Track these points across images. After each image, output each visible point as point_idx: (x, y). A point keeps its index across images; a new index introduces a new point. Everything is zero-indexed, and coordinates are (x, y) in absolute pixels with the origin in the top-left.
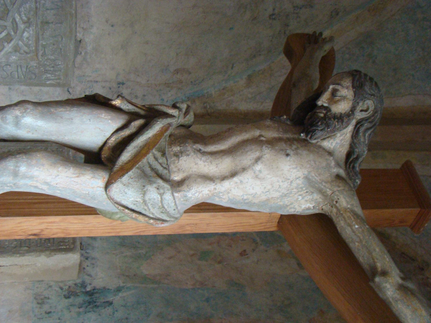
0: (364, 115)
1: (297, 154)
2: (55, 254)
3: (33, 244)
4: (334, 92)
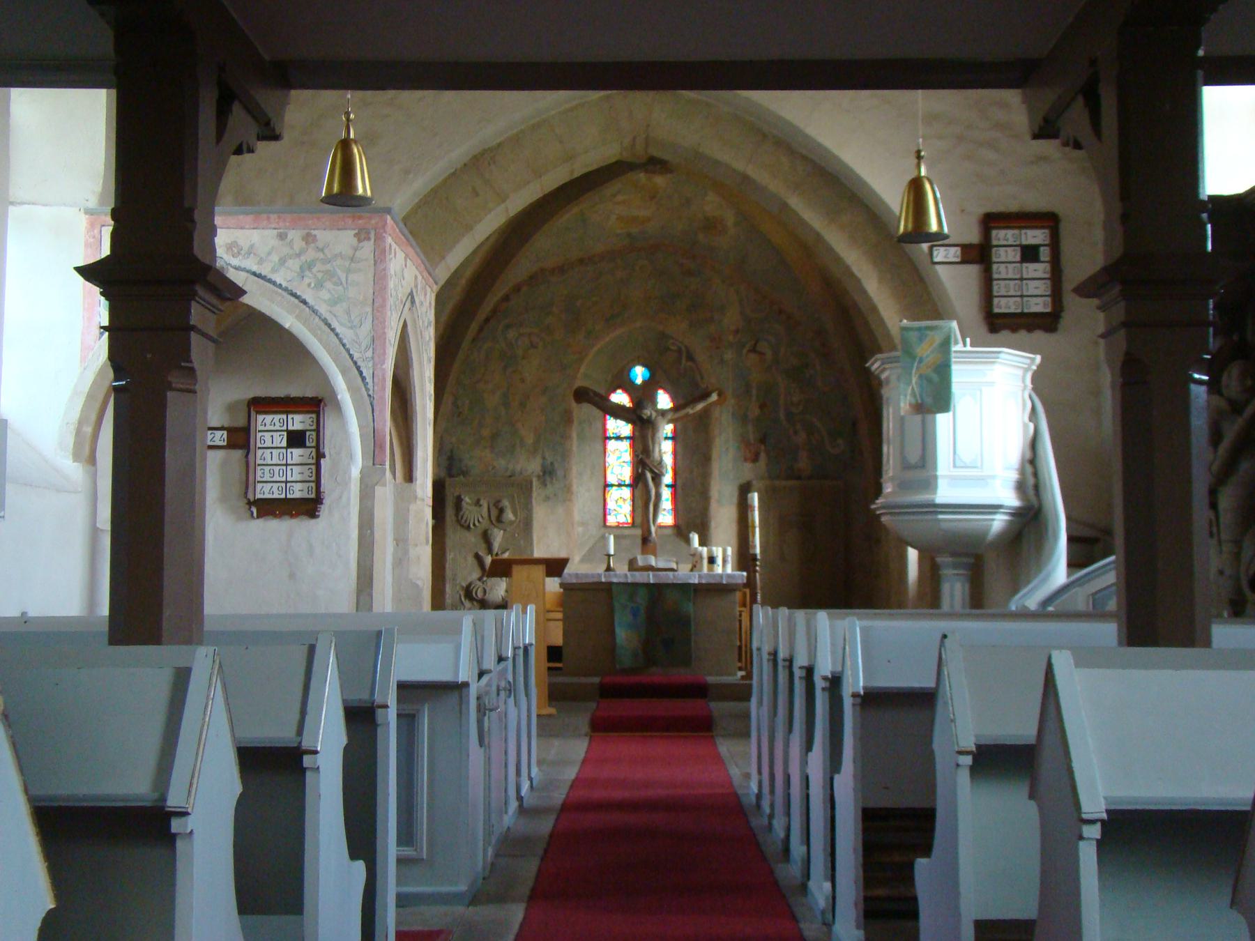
4: (645, 414)
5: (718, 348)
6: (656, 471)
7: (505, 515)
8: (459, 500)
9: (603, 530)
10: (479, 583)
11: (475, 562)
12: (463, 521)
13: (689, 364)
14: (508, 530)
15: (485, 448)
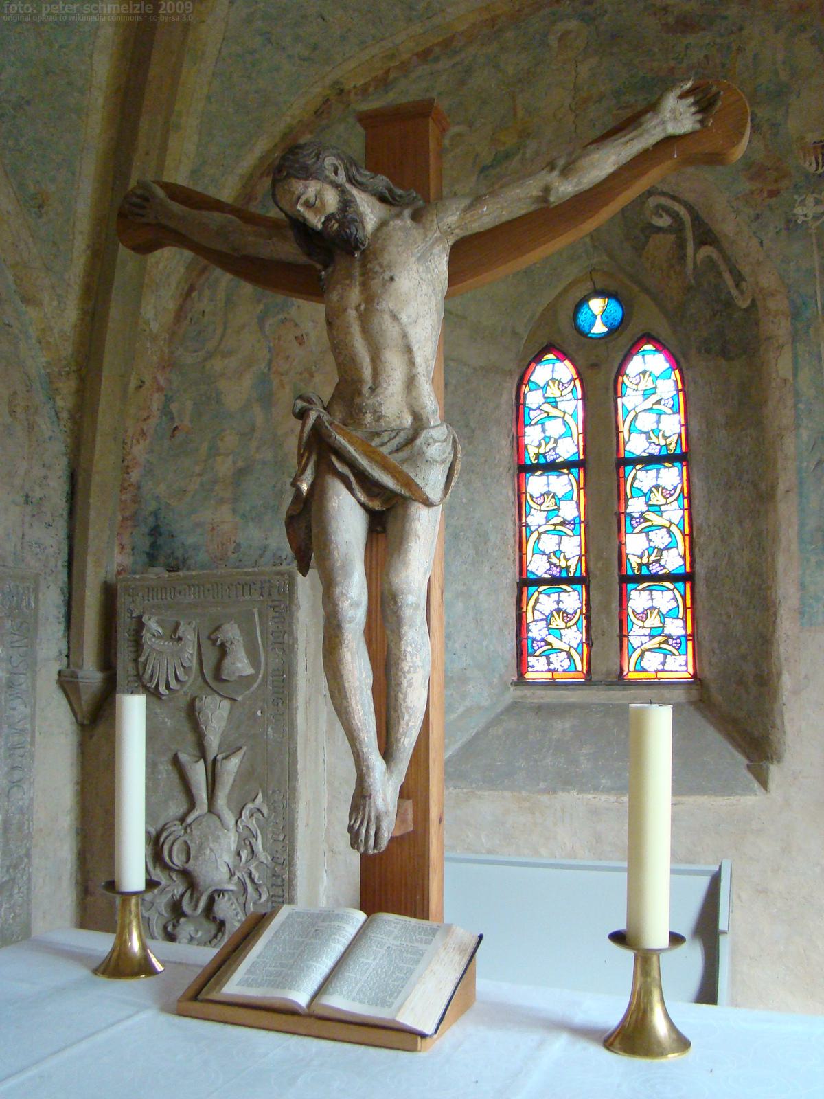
0: (341, 172)
1: (389, 267)
2: (297, 598)
3: (280, 627)
4: (308, 205)
5: (773, 193)
6: (388, 481)
7: (227, 662)
8: (140, 625)
9: (513, 694)
10: (178, 829)
11: (175, 777)
12: (147, 676)
13: (706, 251)
14: (239, 698)
15: (222, 501)
